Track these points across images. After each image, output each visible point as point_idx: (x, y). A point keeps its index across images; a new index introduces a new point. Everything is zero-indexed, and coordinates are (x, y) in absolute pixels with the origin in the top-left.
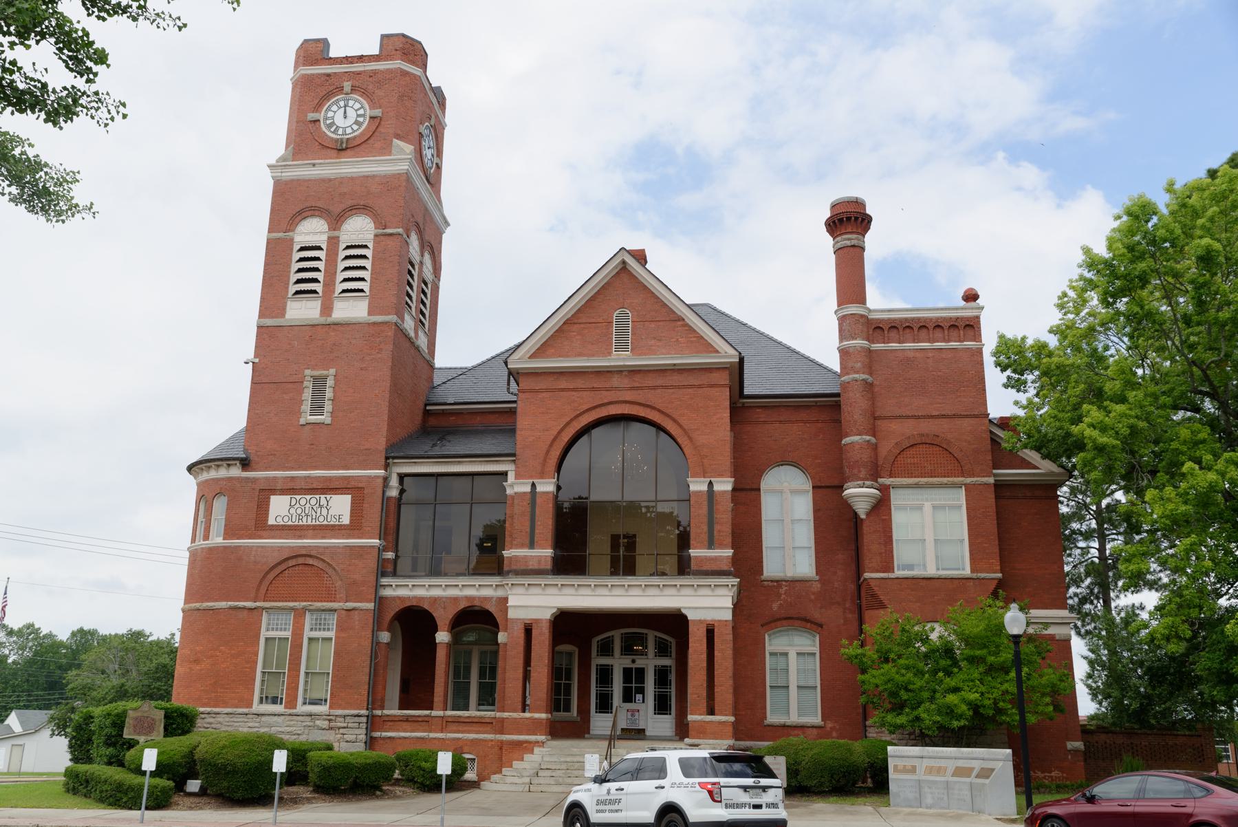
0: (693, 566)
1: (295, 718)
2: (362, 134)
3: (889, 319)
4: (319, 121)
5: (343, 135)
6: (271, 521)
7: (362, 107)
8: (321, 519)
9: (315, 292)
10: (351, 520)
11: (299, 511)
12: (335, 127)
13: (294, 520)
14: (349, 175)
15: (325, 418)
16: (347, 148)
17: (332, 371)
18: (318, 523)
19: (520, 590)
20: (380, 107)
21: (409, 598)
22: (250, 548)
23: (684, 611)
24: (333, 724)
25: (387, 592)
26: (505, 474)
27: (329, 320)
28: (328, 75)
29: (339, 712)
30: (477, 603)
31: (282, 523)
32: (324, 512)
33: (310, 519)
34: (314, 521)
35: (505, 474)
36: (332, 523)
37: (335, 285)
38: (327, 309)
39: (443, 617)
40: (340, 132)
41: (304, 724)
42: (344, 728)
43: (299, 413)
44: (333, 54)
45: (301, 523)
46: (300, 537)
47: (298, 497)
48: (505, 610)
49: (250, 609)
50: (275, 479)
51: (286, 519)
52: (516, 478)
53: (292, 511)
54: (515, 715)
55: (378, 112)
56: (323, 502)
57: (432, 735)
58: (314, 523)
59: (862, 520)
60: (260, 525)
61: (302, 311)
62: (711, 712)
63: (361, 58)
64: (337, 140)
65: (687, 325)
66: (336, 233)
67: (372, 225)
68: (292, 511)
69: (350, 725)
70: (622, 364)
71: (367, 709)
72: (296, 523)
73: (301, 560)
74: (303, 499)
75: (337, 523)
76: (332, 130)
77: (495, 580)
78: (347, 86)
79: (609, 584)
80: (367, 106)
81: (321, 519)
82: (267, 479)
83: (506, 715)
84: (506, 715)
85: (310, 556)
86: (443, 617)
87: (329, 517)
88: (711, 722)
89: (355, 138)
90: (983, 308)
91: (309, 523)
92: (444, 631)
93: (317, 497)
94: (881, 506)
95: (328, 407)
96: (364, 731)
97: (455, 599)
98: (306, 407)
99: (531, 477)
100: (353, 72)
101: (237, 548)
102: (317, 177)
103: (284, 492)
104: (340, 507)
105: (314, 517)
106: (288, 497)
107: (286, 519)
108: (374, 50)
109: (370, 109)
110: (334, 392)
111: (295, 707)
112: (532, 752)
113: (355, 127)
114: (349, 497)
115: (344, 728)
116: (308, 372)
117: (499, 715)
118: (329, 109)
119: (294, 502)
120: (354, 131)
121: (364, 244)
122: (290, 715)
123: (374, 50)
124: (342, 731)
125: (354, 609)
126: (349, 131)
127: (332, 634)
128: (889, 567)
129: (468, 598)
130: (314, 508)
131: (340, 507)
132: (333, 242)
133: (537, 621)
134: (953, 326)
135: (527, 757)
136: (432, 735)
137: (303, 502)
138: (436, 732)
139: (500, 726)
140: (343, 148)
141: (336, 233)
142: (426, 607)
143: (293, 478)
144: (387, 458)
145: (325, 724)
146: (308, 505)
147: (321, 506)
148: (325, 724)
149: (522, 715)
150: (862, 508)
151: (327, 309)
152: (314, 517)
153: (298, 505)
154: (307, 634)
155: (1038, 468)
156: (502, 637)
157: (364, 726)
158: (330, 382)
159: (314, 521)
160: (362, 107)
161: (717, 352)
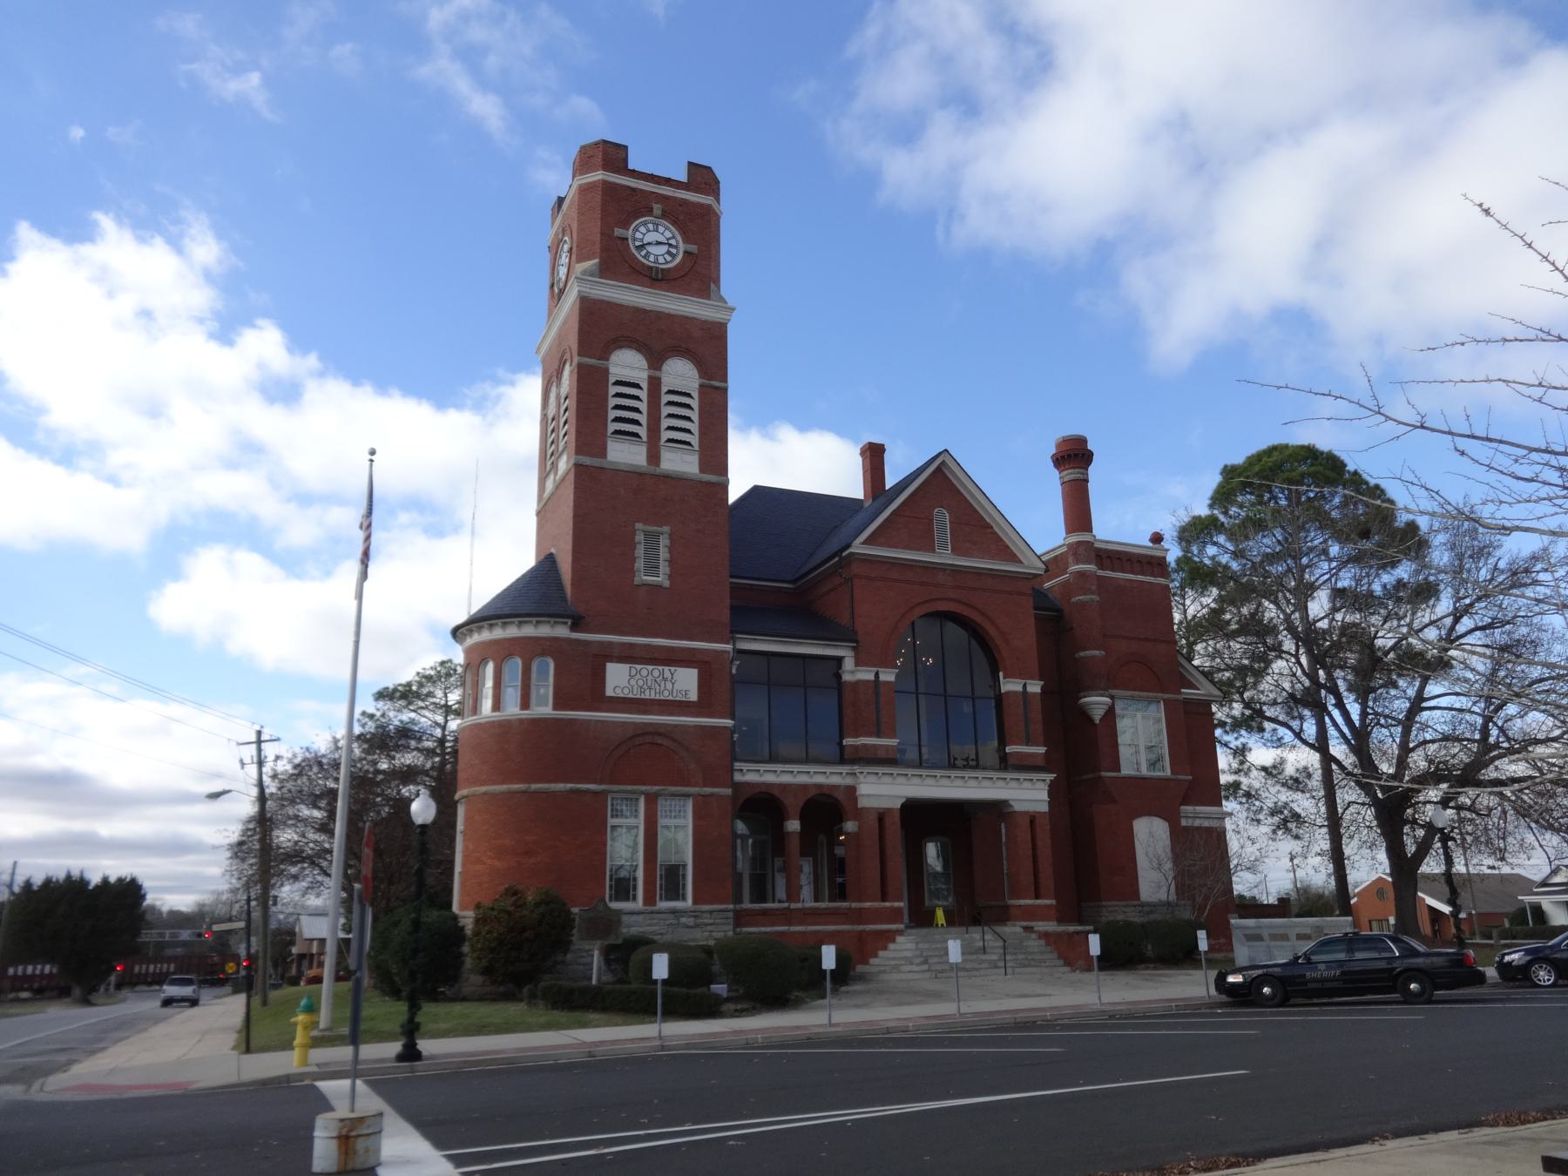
0: (1011, 761)
1: (656, 916)
3: (1106, 550)
4: (627, 239)
5: (654, 262)
6: (609, 692)
7: (674, 237)
8: (666, 693)
9: (636, 435)
10: (699, 697)
11: (641, 682)
12: (645, 251)
13: (635, 693)
14: (666, 311)
15: (662, 578)
16: (662, 280)
17: (666, 529)
18: (662, 698)
19: (872, 778)
23: (1012, 803)
24: (699, 921)
25: (738, 777)
26: (839, 661)
27: (658, 471)
28: (634, 190)
29: (705, 907)
33: (653, 692)
34: (658, 695)
35: (839, 661)
36: (678, 699)
37: (660, 432)
38: (654, 457)
40: (652, 258)
41: (667, 922)
42: (711, 924)
45: (643, 696)
46: (645, 712)
47: (639, 667)
48: (855, 799)
49: (595, 793)
50: (610, 644)
51: (626, 691)
52: (857, 664)
53: (633, 682)
55: (693, 248)
56: (668, 674)
58: (658, 697)
59: (1096, 725)
60: (596, 696)
61: (625, 454)
63: (668, 182)
65: (995, 533)
66: (657, 374)
67: (695, 373)
68: (633, 682)
70: (951, 562)
71: (733, 903)
72: (638, 696)
73: (648, 739)
74: (645, 669)
75: (684, 699)
76: (643, 253)
77: (845, 769)
78: (657, 208)
79: (939, 775)
80: (679, 238)
81: (666, 693)
82: (601, 643)
83: (867, 905)
84: (867, 905)
85: (660, 734)
86: (793, 804)
87: (675, 691)
88: (1039, 906)
89: (669, 269)
90: (1168, 550)
91: (653, 697)
92: (795, 819)
93: (660, 668)
94: (1110, 714)
95: (664, 568)
96: (731, 927)
97: (805, 787)
98: (640, 564)
99: (874, 666)
100: (661, 195)
101: (572, 721)
102: (631, 304)
104: (686, 682)
105: (658, 691)
106: (627, 666)
107: (626, 691)
108: (681, 175)
109: (684, 242)
110: (670, 552)
111: (654, 904)
112: (893, 941)
113: (669, 258)
114: (695, 671)
115: (711, 924)
116: (639, 526)
117: (854, 905)
118: (636, 229)
120: (667, 262)
121: (687, 392)
122: (652, 912)
123: (681, 175)
124: (709, 928)
125: (712, 795)
126: (661, 260)
128: (1117, 768)
129: (819, 786)
130: (658, 680)
131: (686, 682)
132: (655, 384)
134: (1149, 563)
135: (891, 946)
137: (644, 673)
139: (860, 916)
140: (656, 278)
141: (657, 374)
142: (776, 793)
143: (631, 645)
144: (732, 632)
145: (691, 921)
146: (650, 677)
147: (665, 680)
148: (691, 921)
150: (1097, 714)
151: (654, 457)
152: (658, 691)
153: (638, 676)
155: (1199, 690)
157: (731, 921)
158: (664, 541)
159: (658, 695)
161: (1021, 562)
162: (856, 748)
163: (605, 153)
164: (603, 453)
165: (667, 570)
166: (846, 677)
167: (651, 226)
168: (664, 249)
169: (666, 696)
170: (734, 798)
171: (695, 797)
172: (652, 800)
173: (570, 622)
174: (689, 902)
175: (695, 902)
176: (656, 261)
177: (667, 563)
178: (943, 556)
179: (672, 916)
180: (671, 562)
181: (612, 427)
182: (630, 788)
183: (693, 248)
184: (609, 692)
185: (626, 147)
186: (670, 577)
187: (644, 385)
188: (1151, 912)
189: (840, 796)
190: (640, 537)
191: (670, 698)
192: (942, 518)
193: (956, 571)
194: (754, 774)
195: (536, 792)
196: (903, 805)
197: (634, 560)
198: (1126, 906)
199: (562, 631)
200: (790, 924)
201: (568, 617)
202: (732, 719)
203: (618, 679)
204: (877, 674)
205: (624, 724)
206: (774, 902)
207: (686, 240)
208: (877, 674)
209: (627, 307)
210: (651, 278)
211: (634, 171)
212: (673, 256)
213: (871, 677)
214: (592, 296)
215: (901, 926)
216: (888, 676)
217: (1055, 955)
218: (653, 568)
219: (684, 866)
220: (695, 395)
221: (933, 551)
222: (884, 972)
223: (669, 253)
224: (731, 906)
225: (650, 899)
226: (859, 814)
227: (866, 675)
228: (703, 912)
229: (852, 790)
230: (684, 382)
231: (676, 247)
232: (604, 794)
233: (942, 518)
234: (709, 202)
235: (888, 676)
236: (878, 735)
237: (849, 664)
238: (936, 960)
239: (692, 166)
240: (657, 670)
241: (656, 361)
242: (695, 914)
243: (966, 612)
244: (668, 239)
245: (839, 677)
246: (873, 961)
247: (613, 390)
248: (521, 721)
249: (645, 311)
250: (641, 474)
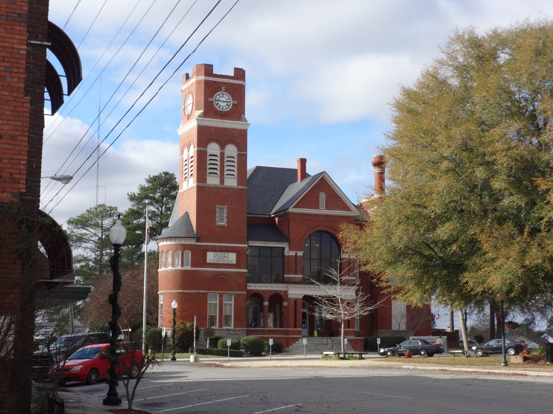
1: (222, 331)
2: (230, 110)
5: (222, 109)
6: (208, 261)
7: (229, 98)
8: (226, 261)
10: (236, 262)
11: (218, 258)
12: (219, 105)
14: (226, 127)
15: (224, 223)
17: (226, 206)
19: (293, 288)
21: (255, 290)
22: (201, 271)
25: (248, 288)
26: (283, 249)
27: (223, 186)
28: (215, 82)
29: (237, 329)
30: (277, 292)
31: (212, 262)
32: (227, 259)
33: (222, 261)
35: (284, 248)
38: (222, 181)
39: (267, 297)
40: (221, 108)
41: (226, 333)
43: (215, 222)
44: (215, 72)
45: (218, 263)
46: (219, 268)
47: (217, 253)
48: (287, 295)
49: (204, 293)
50: (208, 246)
51: (213, 261)
53: (215, 258)
54: (292, 329)
55: (236, 102)
56: (226, 255)
60: (204, 263)
61: (213, 181)
65: (342, 200)
66: (223, 151)
68: (215, 258)
69: (241, 333)
77: (284, 285)
78: (223, 88)
80: (231, 98)
81: (226, 261)
82: (205, 246)
83: (290, 329)
84: (290, 329)
85: (224, 275)
86: (267, 297)
89: (227, 111)
91: (221, 263)
93: (224, 253)
95: (225, 220)
97: (270, 291)
98: (217, 219)
101: (196, 271)
103: (212, 251)
104: (232, 258)
106: (214, 253)
107: (213, 261)
108: (232, 74)
110: (227, 214)
111: (222, 327)
112: (298, 340)
113: (227, 107)
114: (235, 254)
116: (217, 206)
117: (285, 329)
119: (215, 255)
120: (227, 108)
122: (221, 330)
123: (232, 74)
124: (238, 335)
125: (240, 294)
126: (225, 108)
127: (233, 302)
131: (232, 258)
132: (222, 155)
133: (298, 299)
135: (297, 342)
136: (265, 336)
137: (219, 255)
139: (287, 333)
141: (223, 151)
143: (215, 246)
145: (233, 333)
146: (221, 256)
147: (225, 257)
148: (233, 333)
149: (295, 329)
151: (222, 181)
153: (217, 256)
154: (224, 302)
156: (285, 304)
158: (225, 211)
160: (229, 98)
161: (351, 211)
162: (288, 278)
163: (205, 69)
164: (205, 181)
165: (226, 220)
166: (286, 254)
167: (221, 95)
168: (225, 103)
169: (226, 262)
170: (247, 295)
171: (235, 294)
172: (221, 296)
173: (196, 239)
174: (232, 327)
175: (234, 327)
176: (223, 109)
177: (226, 218)
178: (322, 211)
179: (227, 331)
180: (228, 218)
181: (209, 171)
182: (214, 292)
183: (236, 102)
184: (208, 261)
185: (212, 65)
186: (228, 223)
187: (219, 155)
188: (395, 334)
189: (282, 294)
190: (217, 210)
191: (227, 263)
192: (322, 196)
193: (327, 216)
194: (253, 287)
195: (186, 293)
196: (303, 297)
197: (215, 217)
198: (387, 331)
199: (193, 242)
200: (264, 335)
201: (195, 238)
202: (247, 269)
203: (211, 257)
204: (296, 253)
205: (212, 272)
206: (260, 327)
207: (234, 99)
208: (296, 253)
209: (213, 127)
210: (221, 116)
211: (215, 74)
212: (229, 106)
213: (294, 254)
214: (201, 125)
215: (301, 336)
216: (300, 254)
217: (351, 347)
218: (222, 220)
219: (231, 316)
220: (236, 157)
221: (318, 208)
222: (294, 350)
223: (227, 105)
224: (246, 329)
225: (220, 326)
226: (288, 300)
227: (292, 253)
228: (237, 330)
229: (286, 292)
230: (232, 153)
231: (230, 102)
232: (206, 294)
233: (322, 196)
234: (241, 83)
235: (300, 254)
236: (296, 274)
237: (287, 249)
238: (310, 347)
239: (236, 70)
240: (222, 254)
241: (223, 147)
242: (234, 331)
243: (329, 230)
244: (227, 99)
245: (283, 254)
246: (291, 347)
247: (209, 158)
248: (181, 271)
249: (219, 128)
250: (218, 188)
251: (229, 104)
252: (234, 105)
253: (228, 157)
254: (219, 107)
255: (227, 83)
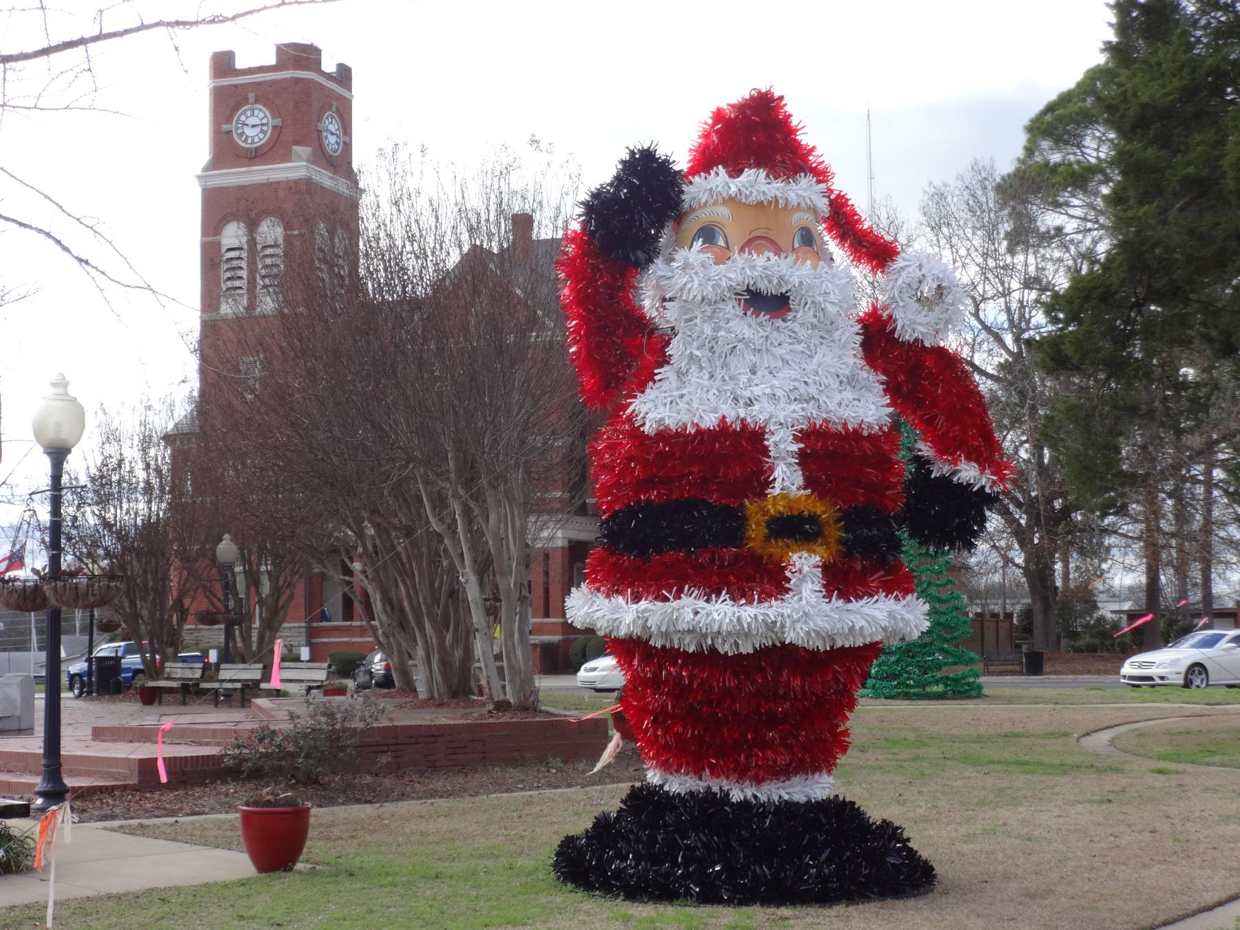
2: (267, 142)
16: (255, 157)
20: (280, 117)
28: (236, 86)
40: (249, 141)
44: (239, 65)
57: (354, 640)
62: (547, 615)
63: (261, 69)
64: (247, 149)
78: (251, 96)
80: (269, 116)
88: (547, 623)
96: (304, 638)
108: (271, 60)
113: (261, 136)
120: (261, 140)
123: (271, 60)
126: (256, 139)
136: (354, 640)
138: (355, 637)
157: (304, 634)
160: (265, 116)
164: (218, 309)
167: (249, 113)
168: (257, 130)
176: (253, 142)
200: (352, 637)
207: (274, 117)
209: (233, 187)
223: (262, 131)
231: (267, 124)
241: (252, 226)
249: (245, 187)
251: (265, 128)
252: (274, 127)
253: (264, 248)
254: (265, 134)
255: (259, 84)
